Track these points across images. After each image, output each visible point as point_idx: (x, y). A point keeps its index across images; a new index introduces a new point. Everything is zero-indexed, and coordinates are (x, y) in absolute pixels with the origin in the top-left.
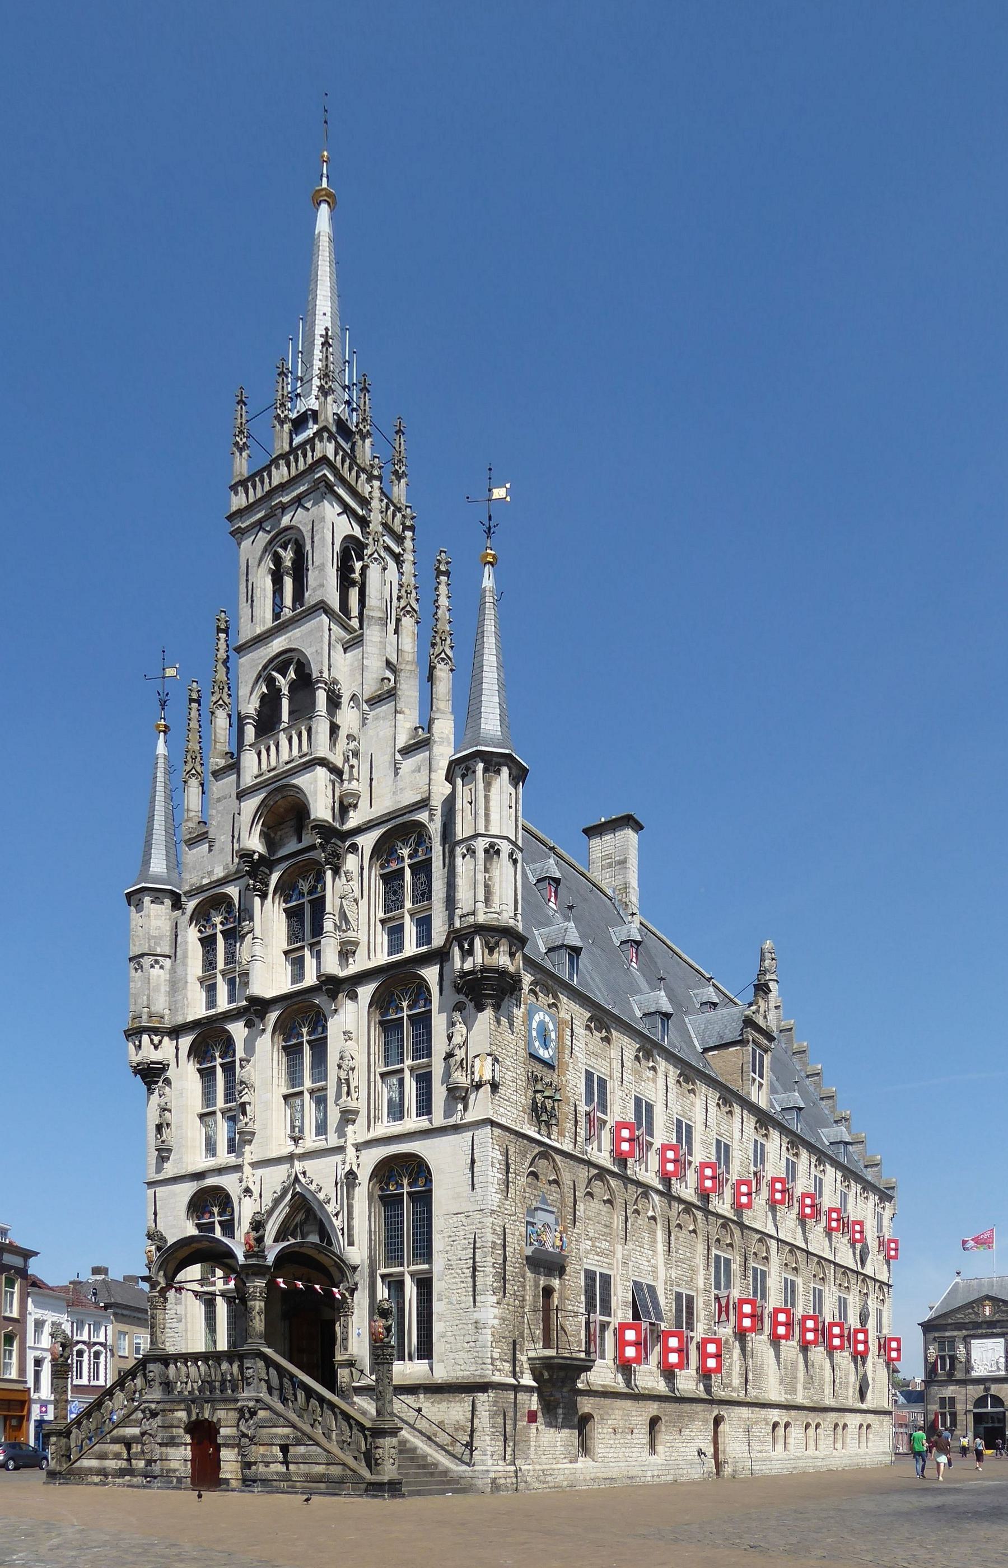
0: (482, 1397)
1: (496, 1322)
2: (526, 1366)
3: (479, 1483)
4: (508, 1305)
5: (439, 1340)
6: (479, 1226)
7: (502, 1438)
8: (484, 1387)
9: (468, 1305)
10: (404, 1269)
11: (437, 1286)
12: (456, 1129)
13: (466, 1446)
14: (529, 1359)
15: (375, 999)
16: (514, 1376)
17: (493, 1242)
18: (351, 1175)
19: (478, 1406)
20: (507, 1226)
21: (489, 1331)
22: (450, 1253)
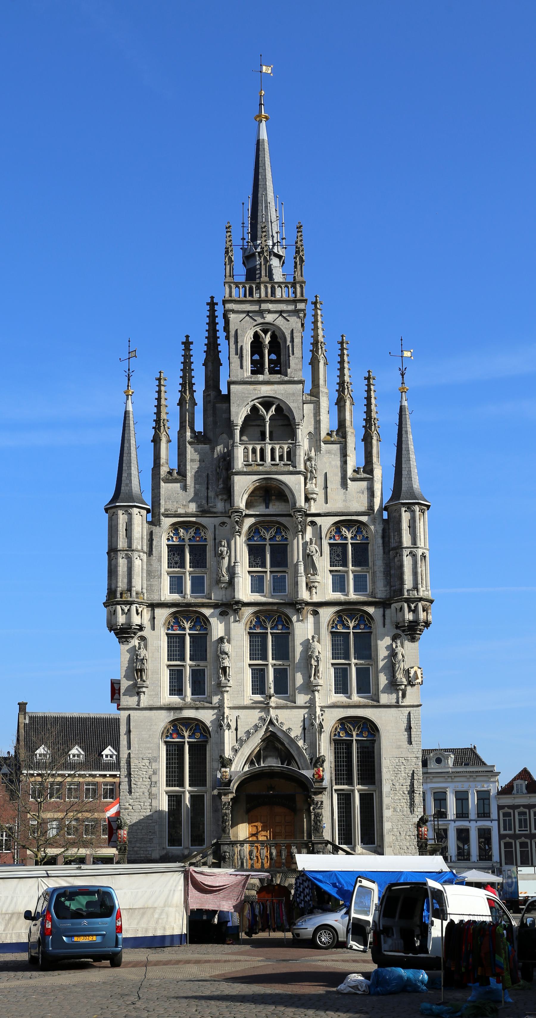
6: (415, 766)
12: (397, 706)
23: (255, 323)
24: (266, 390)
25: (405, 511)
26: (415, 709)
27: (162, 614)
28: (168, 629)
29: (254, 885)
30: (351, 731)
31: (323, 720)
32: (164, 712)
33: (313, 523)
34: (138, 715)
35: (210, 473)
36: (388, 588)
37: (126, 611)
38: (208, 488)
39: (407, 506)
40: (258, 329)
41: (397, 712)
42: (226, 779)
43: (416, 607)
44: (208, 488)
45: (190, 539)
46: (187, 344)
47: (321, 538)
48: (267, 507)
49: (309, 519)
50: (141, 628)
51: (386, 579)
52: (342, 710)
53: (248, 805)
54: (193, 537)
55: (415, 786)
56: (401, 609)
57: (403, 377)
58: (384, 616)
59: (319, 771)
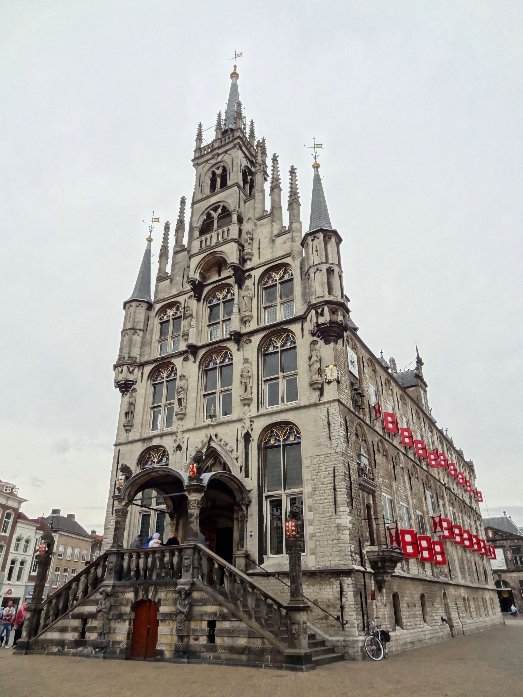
0: (348, 581)
1: (350, 525)
2: (366, 557)
3: (351, 651)
4: (355, 514)
5: (311, 539)
7: (361, 612)
8: (348, 573)
9: (330, 514)
10: (282, 492)
11: (307, 502)
12: (315, 405)
13: (338, 619)
14: (367, 552)
15: (262, 343)
16: (362, 565)
17: (345, 473)
18: (247, 437)
19: (345, 587)
20: (350, 463)
21: (348, 532)
22: (316, 481)
23: (211, 165)
24: (214, 200)
25: (312, 240)
26: (332, 404)
27: (148, 369)
28: (154, 381)
29: (128, 600)
30: (279, 437)
31: (252, 430)
32: (140, 444)
33: (250, 276)
34: (124, 449)
37: (120, 371)
39: (313, 236)
40: (214, 169)
41: (317, 410)
43: (323, 311)
45: (173, 315)
46: (183, 202)
47: (254, 284)
48: (219, 276)
49: (247, 274)
50: (133, 383)
52: (267, 418)
54: (176, 313)
55: (336, 484)
57: (315, 159)
58: (302, 328)
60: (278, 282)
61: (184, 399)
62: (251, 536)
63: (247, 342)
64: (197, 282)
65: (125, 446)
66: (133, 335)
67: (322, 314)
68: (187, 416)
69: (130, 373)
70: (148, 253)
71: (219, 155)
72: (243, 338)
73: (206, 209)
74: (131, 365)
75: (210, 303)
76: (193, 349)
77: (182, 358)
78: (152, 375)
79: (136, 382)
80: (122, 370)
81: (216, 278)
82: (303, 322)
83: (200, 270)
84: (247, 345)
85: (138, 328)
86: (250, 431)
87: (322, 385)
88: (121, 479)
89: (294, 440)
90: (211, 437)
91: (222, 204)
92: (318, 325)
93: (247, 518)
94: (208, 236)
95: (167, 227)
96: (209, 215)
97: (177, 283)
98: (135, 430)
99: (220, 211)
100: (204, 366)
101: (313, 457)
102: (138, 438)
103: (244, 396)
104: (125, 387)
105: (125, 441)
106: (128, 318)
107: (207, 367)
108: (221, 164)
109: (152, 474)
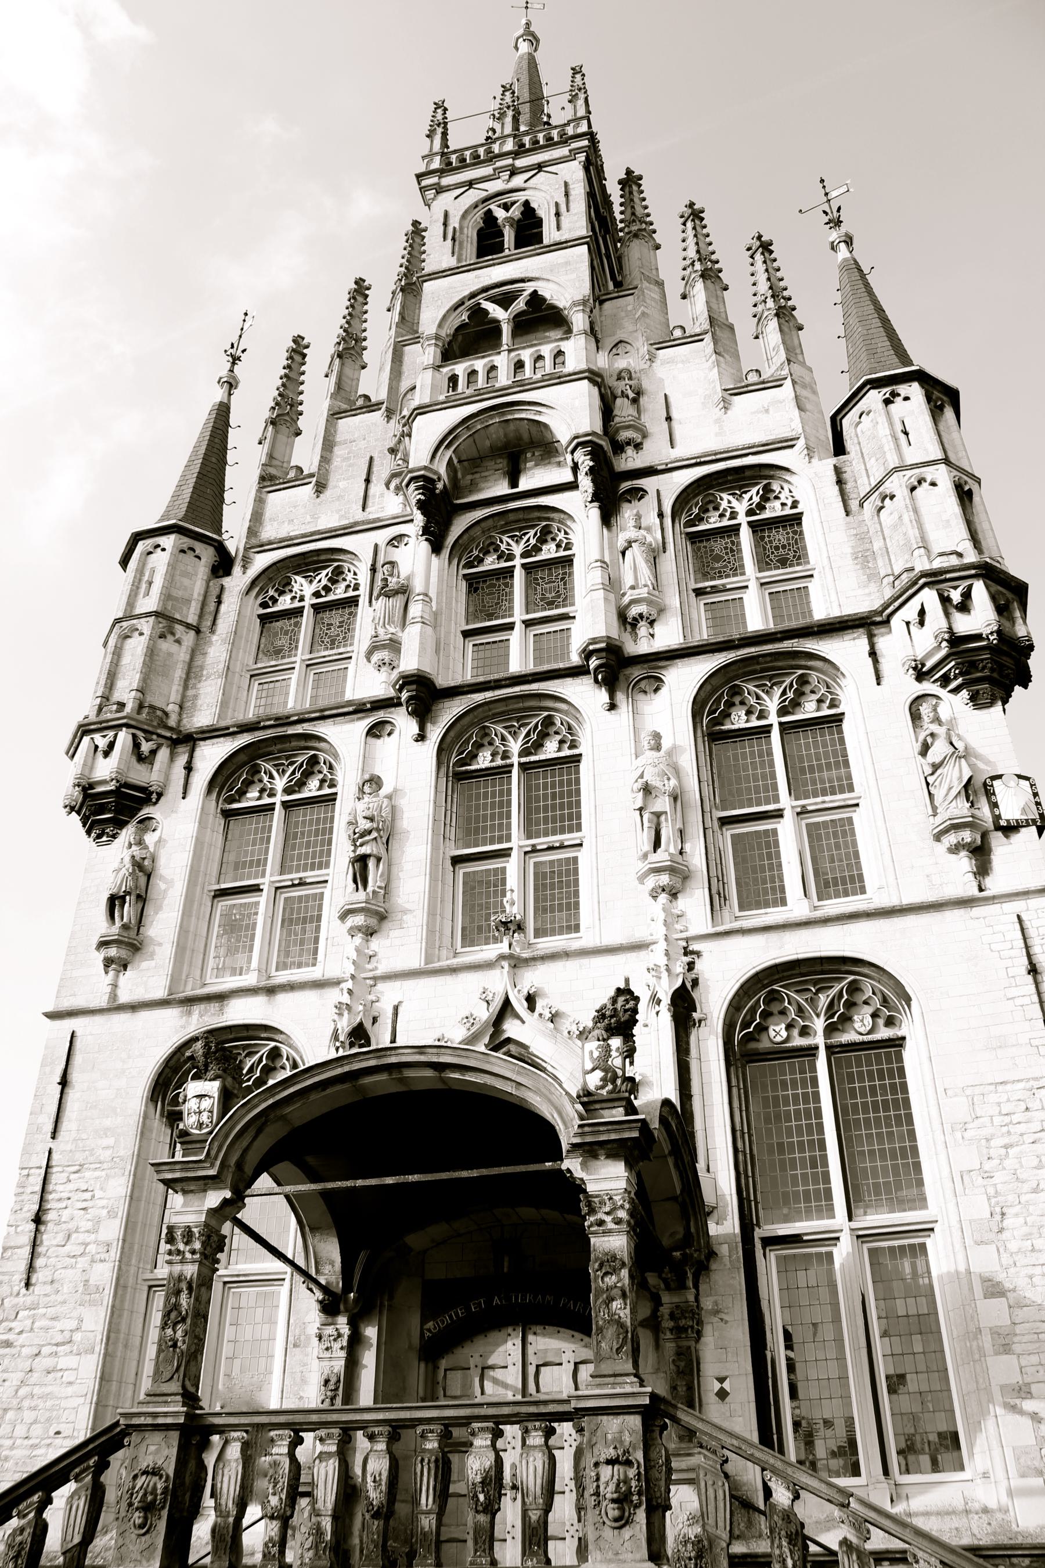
15: (703, 694)
18: (684, 1007)
22: (999, 1177)
25: (887, 402)
27: (211, 756)
28: (231, 800)
31: (695, 982)
35: (376, 456)
36: (873, 587)
38: (368, 481)
39: (888, 389)
42: (200, 1125)
43: (967, 595)
44: (368, 481)
45: (316, 594)
48: (514, 484)
49: (625, 485)
51: (864, 567)
53: (430, 1325)
56: (922, 613)
58: (873, 654)
59: (608, 1050)
60: (742, 519)
61: (379, 859)
62: (722, 1394)
63: (643, 684)
64: (440, 486)
65: (98, 1019)
66: (162, 636)
67: (964, 607)
68: (386, 925)
69: (141, 758)
70: (222, 416)
71: (514, 172)
72: (628, 671)
73: (473, 295)
74: (149, 734)
75: (469, 565)
76: (423, 695)
77: (363, 724)
78: (229, 779)
79: (160, 795)
80: (111, 745)
81: (502, 488)
82: (871, 637)
83: (449, 453)
84: (641, 696)
85: (177, 616)
86: (689, 986)
87: (984, 835)
88: (201, 1097)
89: (869, 1033)
90: (507, 1003)
91: (529, 287)
92: (955, 640)
93: (700, 1322)
94: (480, 365)
95: (298, 351)
96: (478, 313)
97: (339, 498)
98: (145, 965)
99: (520, 304)
100: (453, 760)
101: (978, 1090)
102: (160, 993)
103: (662, 857)
104: (110, 809)
105: (102, 1002)
106: (144, 586)
107: (463, 763)
108: (521, 197)
109: (367, 1080)
